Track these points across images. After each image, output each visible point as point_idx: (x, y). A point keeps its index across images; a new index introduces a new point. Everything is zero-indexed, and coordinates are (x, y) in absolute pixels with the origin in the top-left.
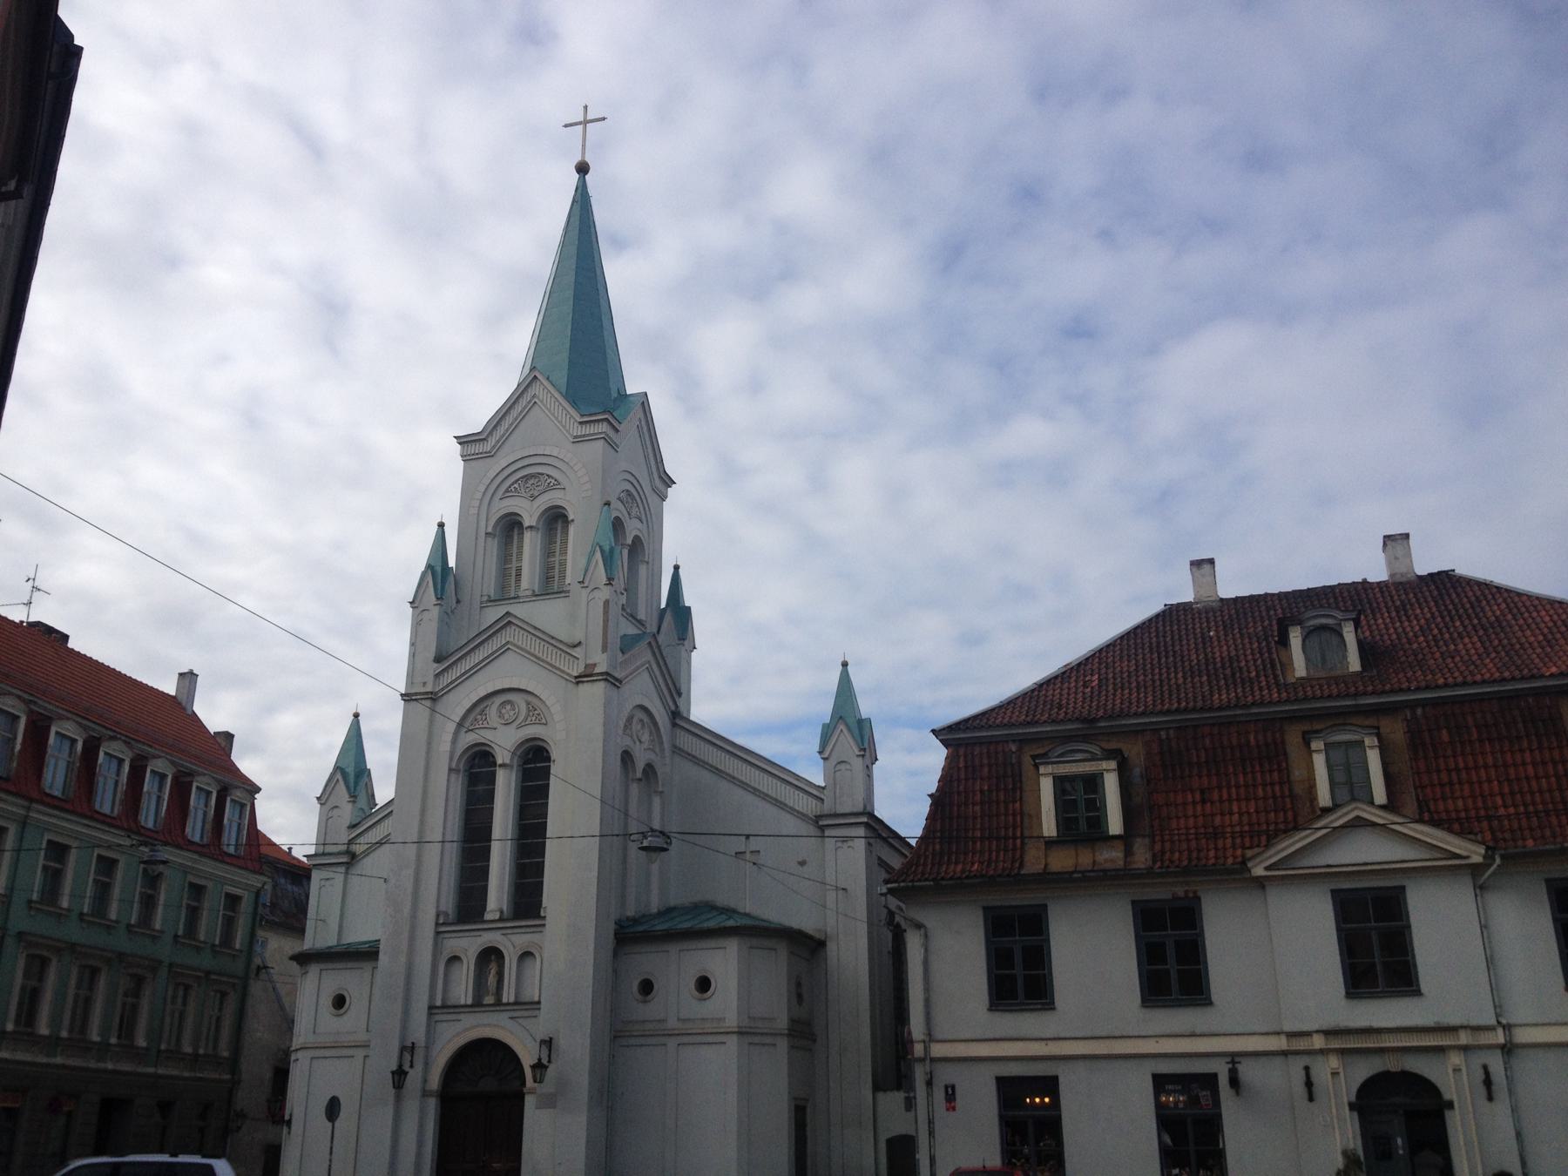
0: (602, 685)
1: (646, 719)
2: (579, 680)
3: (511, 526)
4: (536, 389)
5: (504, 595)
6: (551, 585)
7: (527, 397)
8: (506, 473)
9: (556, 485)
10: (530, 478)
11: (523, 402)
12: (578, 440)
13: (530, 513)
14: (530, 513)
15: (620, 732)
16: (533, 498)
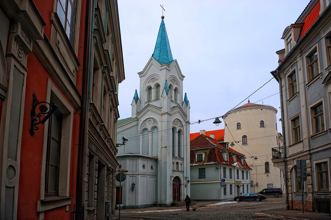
0: (167, 115)
1: (178, 121)
2: (162, 115)
3: (150, 88)
4: (152, 61)
5: (149, 101)
6: (157, 99)
7: (151, 63)
8: (149, 77)
9: (158, 80)
10: (153, 78)
11: (150, 64)
12: (161, 70)
13: (153, 85)
14: (153, 85)
15: (172, 124)
16: (153, 82)
